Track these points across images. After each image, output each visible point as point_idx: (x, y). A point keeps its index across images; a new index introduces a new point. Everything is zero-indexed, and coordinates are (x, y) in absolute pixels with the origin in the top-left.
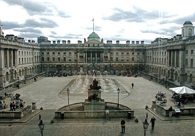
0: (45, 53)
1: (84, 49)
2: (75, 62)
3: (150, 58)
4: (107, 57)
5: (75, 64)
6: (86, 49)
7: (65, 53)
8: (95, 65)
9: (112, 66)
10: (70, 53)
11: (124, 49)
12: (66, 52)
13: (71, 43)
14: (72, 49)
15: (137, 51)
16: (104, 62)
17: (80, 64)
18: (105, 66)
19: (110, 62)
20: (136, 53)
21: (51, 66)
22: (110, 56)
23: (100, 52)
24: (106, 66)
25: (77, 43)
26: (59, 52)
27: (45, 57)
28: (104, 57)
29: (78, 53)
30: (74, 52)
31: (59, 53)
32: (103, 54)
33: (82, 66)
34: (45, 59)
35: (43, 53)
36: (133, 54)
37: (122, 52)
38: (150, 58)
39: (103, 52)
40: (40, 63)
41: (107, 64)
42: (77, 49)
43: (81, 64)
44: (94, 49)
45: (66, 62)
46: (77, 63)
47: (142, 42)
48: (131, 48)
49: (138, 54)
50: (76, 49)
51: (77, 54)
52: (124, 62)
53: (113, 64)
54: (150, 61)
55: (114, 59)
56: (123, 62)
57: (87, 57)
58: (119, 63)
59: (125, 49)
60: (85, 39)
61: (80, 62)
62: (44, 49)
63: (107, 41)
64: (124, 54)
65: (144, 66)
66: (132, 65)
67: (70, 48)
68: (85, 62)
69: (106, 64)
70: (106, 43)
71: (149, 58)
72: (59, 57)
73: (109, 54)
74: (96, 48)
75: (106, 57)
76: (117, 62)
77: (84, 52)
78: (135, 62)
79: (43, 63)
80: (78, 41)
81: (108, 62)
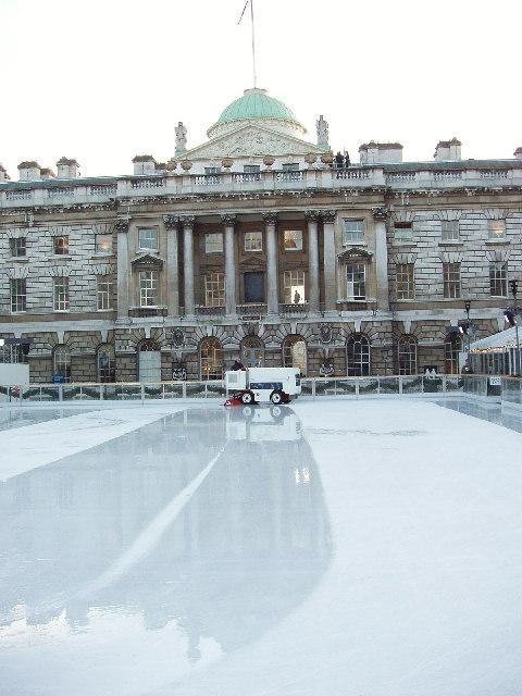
1: (161, 199)
2: (98, 316)
4: (367, 258)
5: (96, 334)
6: (184, 200)
8: (261, 332)
9: (411, 337)
10: (59, 246)
11: (506, 191)
12: (30, 234)
13: (86, 171)
14: (76, 208)
16: (339, 307)
18: (350, 343)
19: (393, 307)
24: (357, 341)
25: (130, 170)
28: (344, 259)
29: (122, 238)
33: (149, 344)
39: (331, 218)
41: (366, 315)
42: (114, 205)
43: (147, 325)
44: (253, 194)
46: (114, 316)
60: (181, 131)
61: (131, 313)
63: (364, 148)
67: (57, 202)
68: (182, 312)
69: (356, 320)
75: (355, 261)
76: (450, 305)
77: (169, 225)
80: (137, 159)
81: (374, 307)
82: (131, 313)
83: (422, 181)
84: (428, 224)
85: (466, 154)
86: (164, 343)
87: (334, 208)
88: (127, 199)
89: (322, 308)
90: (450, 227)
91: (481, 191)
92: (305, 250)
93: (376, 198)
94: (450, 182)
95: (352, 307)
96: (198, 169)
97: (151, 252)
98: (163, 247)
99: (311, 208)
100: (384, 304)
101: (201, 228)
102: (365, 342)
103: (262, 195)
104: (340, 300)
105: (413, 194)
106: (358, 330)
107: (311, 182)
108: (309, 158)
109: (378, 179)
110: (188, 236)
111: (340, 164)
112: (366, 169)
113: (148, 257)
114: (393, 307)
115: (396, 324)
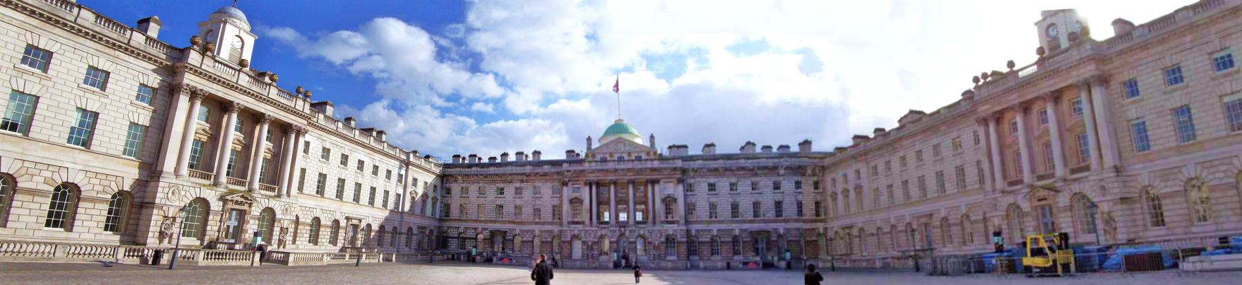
0: (456, 188)
1: (583, 171)
3: (852, 194)
4: (675, 200)
5: (552, 232)
6: (593, 172)
7: (518, 191)
10: (536, 191)
11: (738, 169)
14: (545, 174)
15: (795, 174)
20: (788, 185)
21: (471, 233)
22: (685, 195)
23: (647, 182)
24: (670, 241)
26: (501, 185)
27: (455, 201)
29: (565, 188)
30: (549, 185)
31: (501, 191)
32: (657, 188)
33: (575, 237)
34: (455, 212)
35: (449, 191)
36: (777, 186)
37: (733, 180)
38: (852, 194)
40: (436, 223)
41: (675, 226)
45: (522, 223)
46: (561, 224)
47: (806, 143)
48: (763, 162)
49: (798, 185)
50: (558, 173)
51: (561, 192)
52: (745, 222)
53: (698, 231)
54: (853, 208)
55: (702, 211)
56: (738, 222)
57: (599, 203)
58: (723, 226)
59: (743, 168)
62: (452, 176)
64: (740, 188)
65: (825, 234)
66: (776, 230)
69: (670, 229)
70: (666, 153)
71: (847, 196)
72: (499, 202)
73: (681, 187)
74: (630, 165)
75: (669, 202)
77: (586, 184)
78: (786, 221)
79: (447, 224)
83: (699, 163)
84: (701, 186)
85: (719, 150)
89: (654, 223)
90: (712, 187)
91: (726, 169)
92: (646, 196)
94: (713, 164)
96: (598, 158)
97: (575, 195)
100: (683, 221)
101: (598, 184)
103: (629, 170)
104: (663, 219)
105: (695, 171)
107: (649, 165)
108: (648, 154)
109: (679, 163)
110: (594, 188)
111: (661, 158)
112: (674, 159)
114: (687, 222)
115: (688, 231)
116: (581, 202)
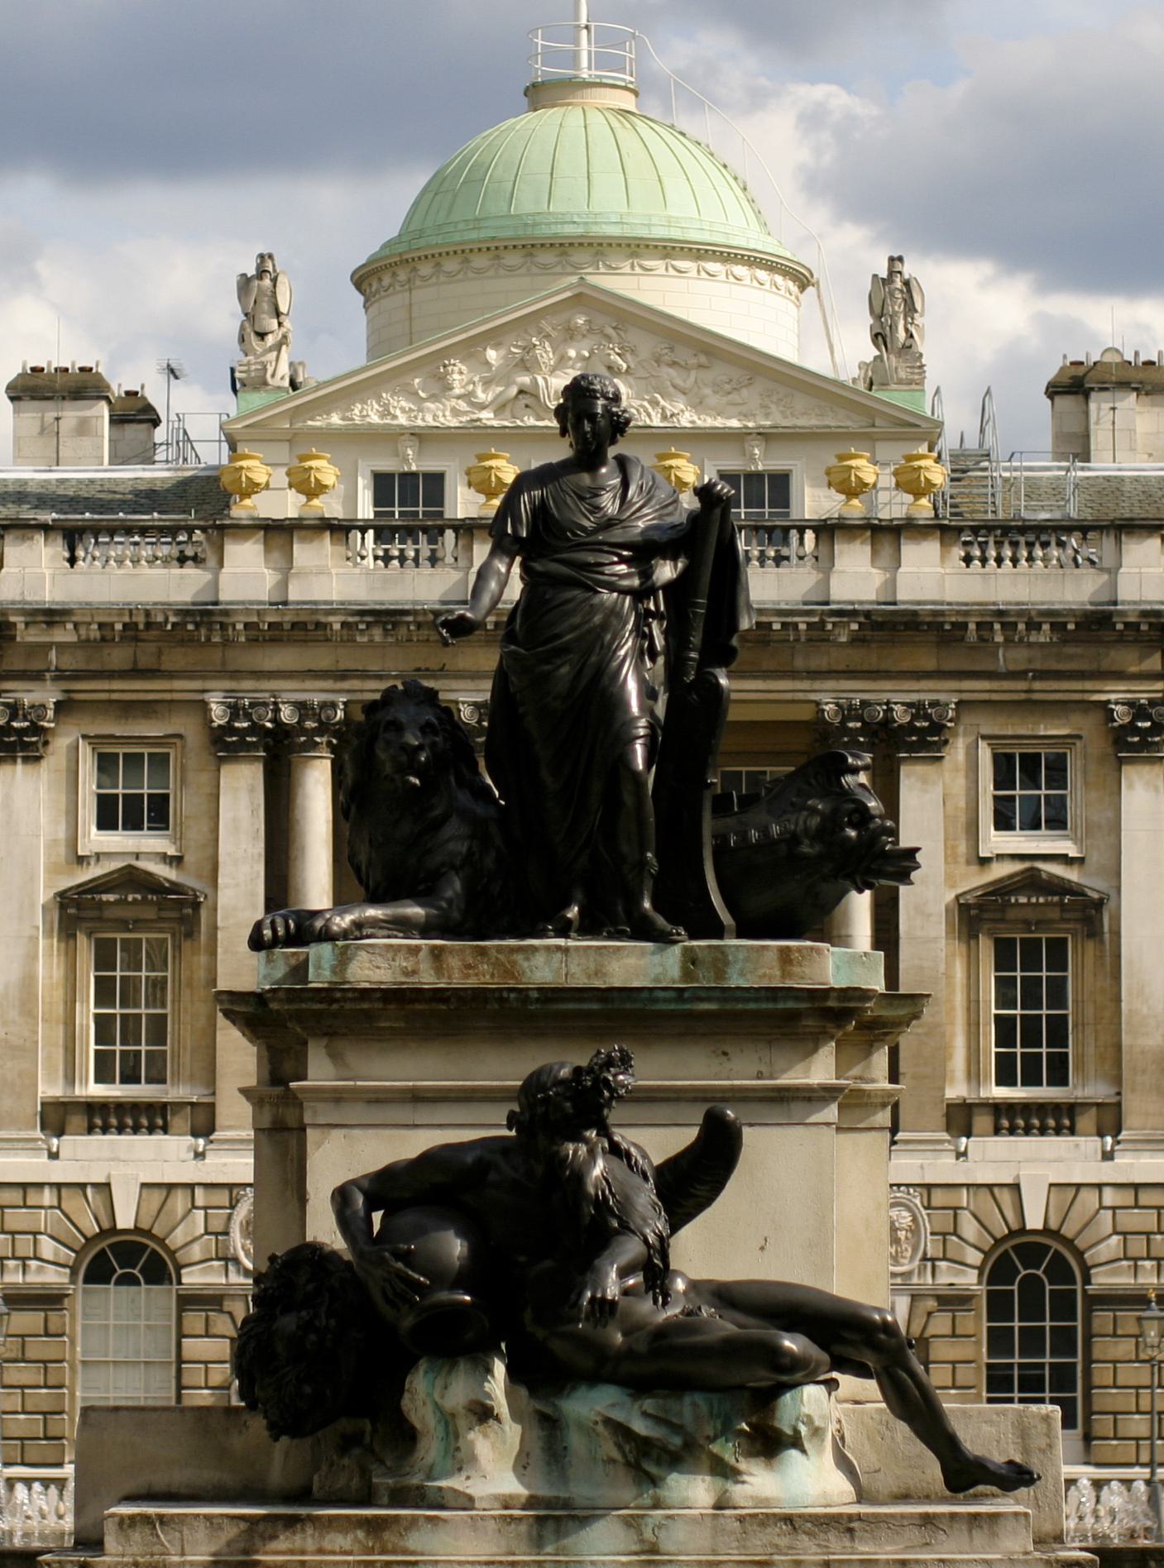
6: (300, 628)
16: (961, 1119)
17: (87, 1156)
18: (998, 1270)
39: (924, 737)
77: (225, 745)
80: (31, 388)
82: (58, 1118)
86: (196, 1252)
87: (945, 693)
88: (52, 616)
93: (1127, 658)
95: (1011, 1119)
98: (196, 833)
99: (858, 691)
102: (1060, 1271)
106: (1034, 1222)
113: (131, 879)
116: (179, 909)
